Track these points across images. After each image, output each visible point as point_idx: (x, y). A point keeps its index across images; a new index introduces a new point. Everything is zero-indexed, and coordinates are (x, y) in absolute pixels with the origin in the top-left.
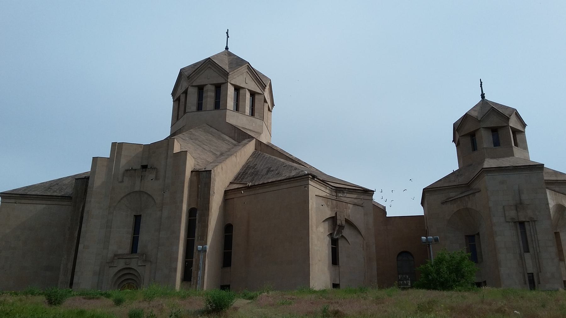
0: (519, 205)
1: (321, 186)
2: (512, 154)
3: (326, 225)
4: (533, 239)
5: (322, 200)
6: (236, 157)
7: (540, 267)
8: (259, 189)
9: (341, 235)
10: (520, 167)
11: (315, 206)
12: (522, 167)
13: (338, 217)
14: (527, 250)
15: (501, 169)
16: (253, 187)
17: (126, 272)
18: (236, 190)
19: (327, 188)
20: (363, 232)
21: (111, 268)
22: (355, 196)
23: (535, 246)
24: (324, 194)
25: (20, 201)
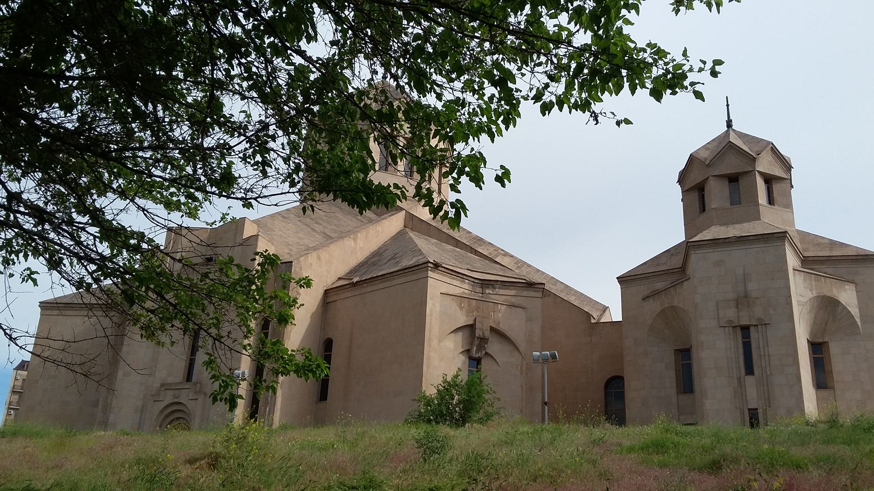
0: (743, 300)
1: (454, 279)
2: (757, 217)
3: (459, 336)
4: (762, 353)
5: (453, 300)
6: (355, 240)
7: (769, 399)
8: (366, 287)
9: (484, 352)
10: (748, 238)
11: (438, 308)
12: (751, 238)
13: (478, 325)
14: (749, 370)
15: (716, 241)
16: (358, 283)
17: (175, 408)
18: (340, 289)
19: (464, 282)
20: (522, 348)
21: (156, 403)
22: (513, 292)
23: (763, 365)
24: (457, 291)
25: (63, 312)
